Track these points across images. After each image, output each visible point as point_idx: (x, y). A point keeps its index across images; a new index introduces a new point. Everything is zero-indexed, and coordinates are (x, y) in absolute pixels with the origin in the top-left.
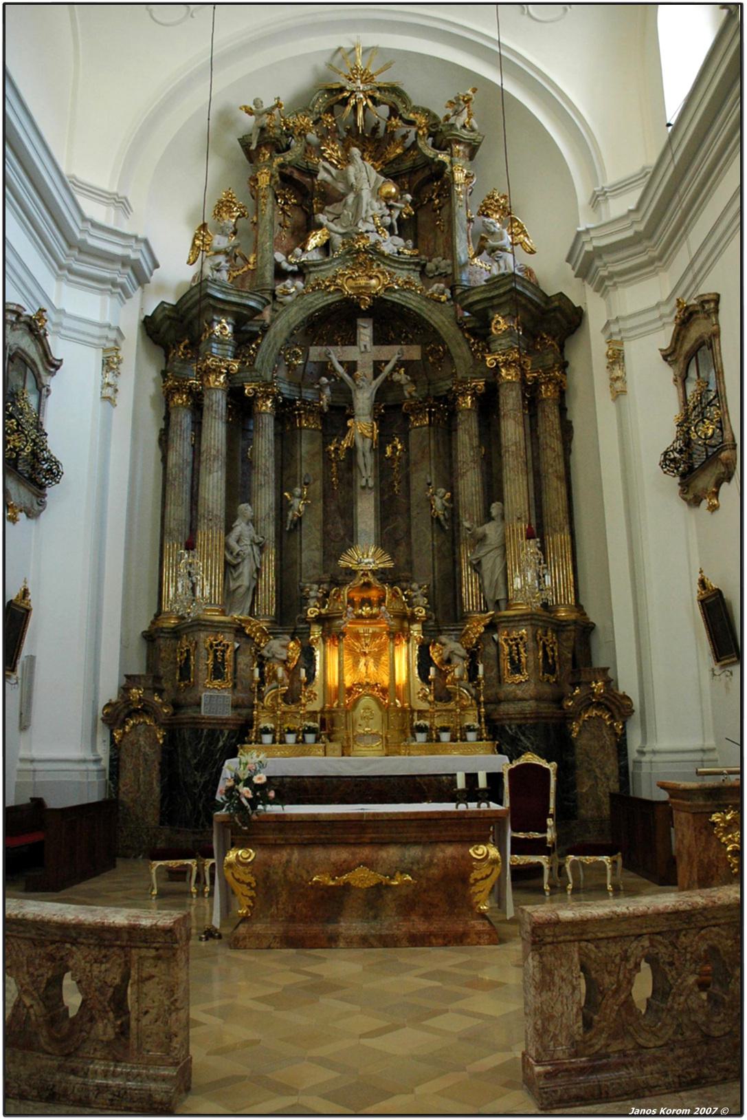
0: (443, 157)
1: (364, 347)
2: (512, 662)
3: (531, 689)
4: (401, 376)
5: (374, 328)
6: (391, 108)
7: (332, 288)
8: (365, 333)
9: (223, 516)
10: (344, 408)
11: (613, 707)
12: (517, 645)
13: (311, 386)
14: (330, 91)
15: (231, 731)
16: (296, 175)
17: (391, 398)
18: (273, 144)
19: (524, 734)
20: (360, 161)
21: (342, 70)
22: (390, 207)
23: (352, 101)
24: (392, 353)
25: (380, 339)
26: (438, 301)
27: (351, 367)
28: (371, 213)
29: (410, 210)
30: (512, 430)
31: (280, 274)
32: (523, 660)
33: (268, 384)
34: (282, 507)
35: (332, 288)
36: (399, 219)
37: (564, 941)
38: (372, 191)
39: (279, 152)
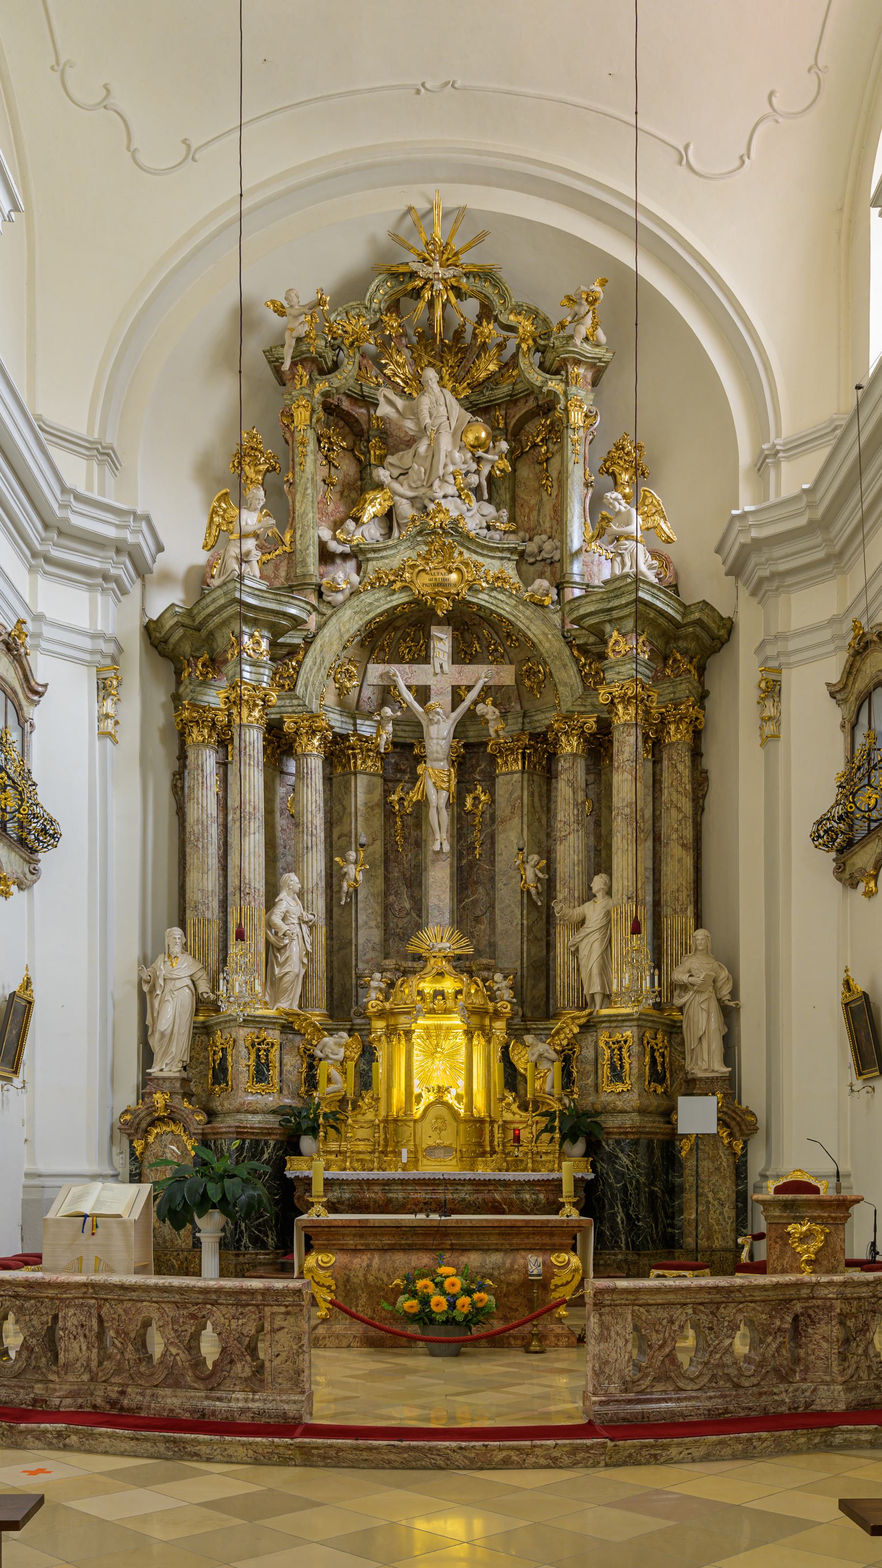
0: (554, 385)
1: (441, 666)
2: (613, 1067)
3: (633, 1100)
4: (488, 710)
5: (454, 639)
6: (483, 306)
7: (398, 585)
8: (442, 643)
9: (263, 890)
10: (411, 746)
11: (733, 1124)
12: (620, 1049)
13: (369, 715)
14: (395, 275)
15: (277, 1142)
16: (346, 405)
17: (473, 736)
18: (314, 360)
19: (622, 1151)
20: (436, 388)
21: (411, 242)
22: (478, 460)
23: (427, 295)
24: (480, 675)
25: (462, 655)
26: (540, 605)
27: (423, 694)
28: (451, 468)
29: (505, 464)
30: (625, 786)
31: (326, 556)
32: (627, 1066)
33: (314, 716)
34: (333, 876)
35: (398, 585)
36: (490, 478)
37: (620, 1305)
38: (454, 435)
39: (322, 372)
